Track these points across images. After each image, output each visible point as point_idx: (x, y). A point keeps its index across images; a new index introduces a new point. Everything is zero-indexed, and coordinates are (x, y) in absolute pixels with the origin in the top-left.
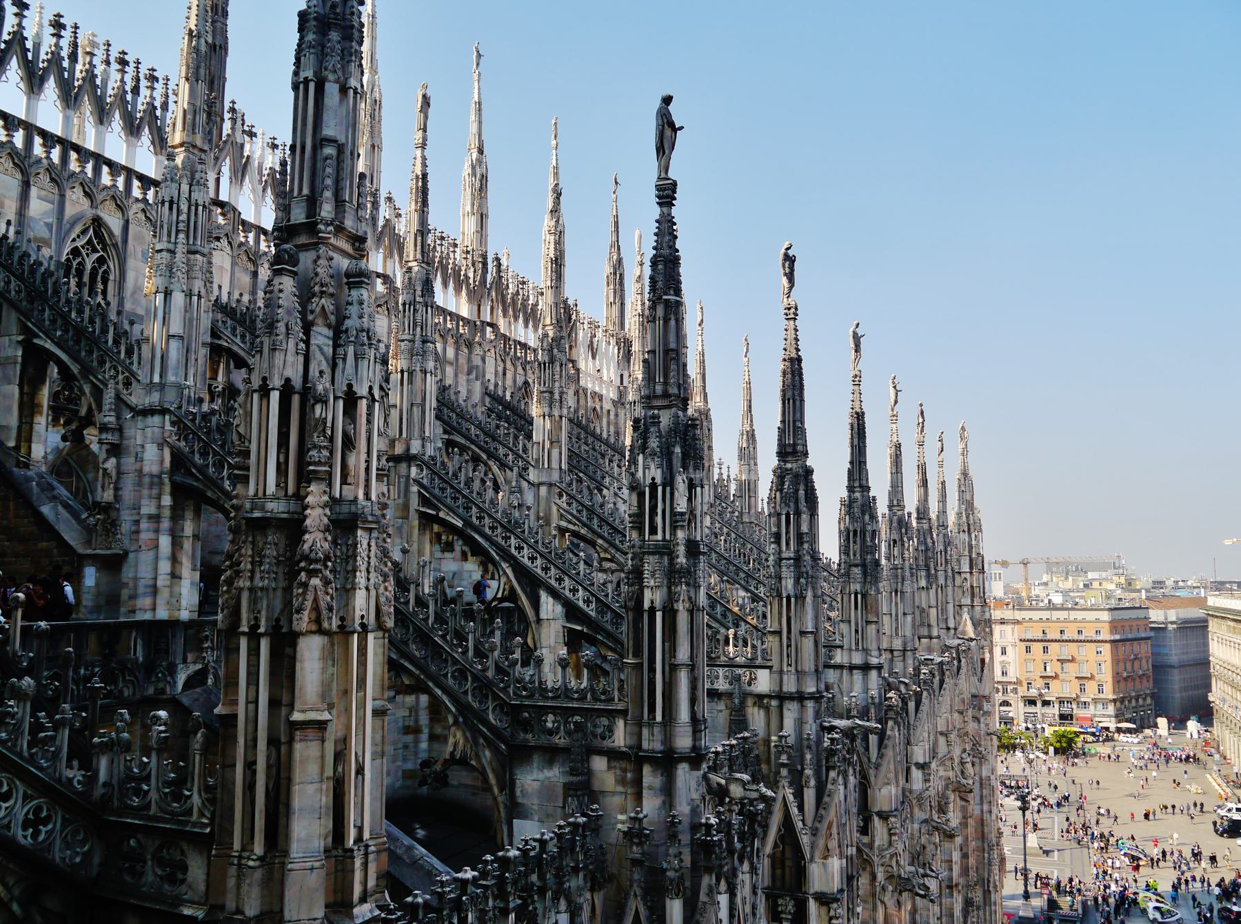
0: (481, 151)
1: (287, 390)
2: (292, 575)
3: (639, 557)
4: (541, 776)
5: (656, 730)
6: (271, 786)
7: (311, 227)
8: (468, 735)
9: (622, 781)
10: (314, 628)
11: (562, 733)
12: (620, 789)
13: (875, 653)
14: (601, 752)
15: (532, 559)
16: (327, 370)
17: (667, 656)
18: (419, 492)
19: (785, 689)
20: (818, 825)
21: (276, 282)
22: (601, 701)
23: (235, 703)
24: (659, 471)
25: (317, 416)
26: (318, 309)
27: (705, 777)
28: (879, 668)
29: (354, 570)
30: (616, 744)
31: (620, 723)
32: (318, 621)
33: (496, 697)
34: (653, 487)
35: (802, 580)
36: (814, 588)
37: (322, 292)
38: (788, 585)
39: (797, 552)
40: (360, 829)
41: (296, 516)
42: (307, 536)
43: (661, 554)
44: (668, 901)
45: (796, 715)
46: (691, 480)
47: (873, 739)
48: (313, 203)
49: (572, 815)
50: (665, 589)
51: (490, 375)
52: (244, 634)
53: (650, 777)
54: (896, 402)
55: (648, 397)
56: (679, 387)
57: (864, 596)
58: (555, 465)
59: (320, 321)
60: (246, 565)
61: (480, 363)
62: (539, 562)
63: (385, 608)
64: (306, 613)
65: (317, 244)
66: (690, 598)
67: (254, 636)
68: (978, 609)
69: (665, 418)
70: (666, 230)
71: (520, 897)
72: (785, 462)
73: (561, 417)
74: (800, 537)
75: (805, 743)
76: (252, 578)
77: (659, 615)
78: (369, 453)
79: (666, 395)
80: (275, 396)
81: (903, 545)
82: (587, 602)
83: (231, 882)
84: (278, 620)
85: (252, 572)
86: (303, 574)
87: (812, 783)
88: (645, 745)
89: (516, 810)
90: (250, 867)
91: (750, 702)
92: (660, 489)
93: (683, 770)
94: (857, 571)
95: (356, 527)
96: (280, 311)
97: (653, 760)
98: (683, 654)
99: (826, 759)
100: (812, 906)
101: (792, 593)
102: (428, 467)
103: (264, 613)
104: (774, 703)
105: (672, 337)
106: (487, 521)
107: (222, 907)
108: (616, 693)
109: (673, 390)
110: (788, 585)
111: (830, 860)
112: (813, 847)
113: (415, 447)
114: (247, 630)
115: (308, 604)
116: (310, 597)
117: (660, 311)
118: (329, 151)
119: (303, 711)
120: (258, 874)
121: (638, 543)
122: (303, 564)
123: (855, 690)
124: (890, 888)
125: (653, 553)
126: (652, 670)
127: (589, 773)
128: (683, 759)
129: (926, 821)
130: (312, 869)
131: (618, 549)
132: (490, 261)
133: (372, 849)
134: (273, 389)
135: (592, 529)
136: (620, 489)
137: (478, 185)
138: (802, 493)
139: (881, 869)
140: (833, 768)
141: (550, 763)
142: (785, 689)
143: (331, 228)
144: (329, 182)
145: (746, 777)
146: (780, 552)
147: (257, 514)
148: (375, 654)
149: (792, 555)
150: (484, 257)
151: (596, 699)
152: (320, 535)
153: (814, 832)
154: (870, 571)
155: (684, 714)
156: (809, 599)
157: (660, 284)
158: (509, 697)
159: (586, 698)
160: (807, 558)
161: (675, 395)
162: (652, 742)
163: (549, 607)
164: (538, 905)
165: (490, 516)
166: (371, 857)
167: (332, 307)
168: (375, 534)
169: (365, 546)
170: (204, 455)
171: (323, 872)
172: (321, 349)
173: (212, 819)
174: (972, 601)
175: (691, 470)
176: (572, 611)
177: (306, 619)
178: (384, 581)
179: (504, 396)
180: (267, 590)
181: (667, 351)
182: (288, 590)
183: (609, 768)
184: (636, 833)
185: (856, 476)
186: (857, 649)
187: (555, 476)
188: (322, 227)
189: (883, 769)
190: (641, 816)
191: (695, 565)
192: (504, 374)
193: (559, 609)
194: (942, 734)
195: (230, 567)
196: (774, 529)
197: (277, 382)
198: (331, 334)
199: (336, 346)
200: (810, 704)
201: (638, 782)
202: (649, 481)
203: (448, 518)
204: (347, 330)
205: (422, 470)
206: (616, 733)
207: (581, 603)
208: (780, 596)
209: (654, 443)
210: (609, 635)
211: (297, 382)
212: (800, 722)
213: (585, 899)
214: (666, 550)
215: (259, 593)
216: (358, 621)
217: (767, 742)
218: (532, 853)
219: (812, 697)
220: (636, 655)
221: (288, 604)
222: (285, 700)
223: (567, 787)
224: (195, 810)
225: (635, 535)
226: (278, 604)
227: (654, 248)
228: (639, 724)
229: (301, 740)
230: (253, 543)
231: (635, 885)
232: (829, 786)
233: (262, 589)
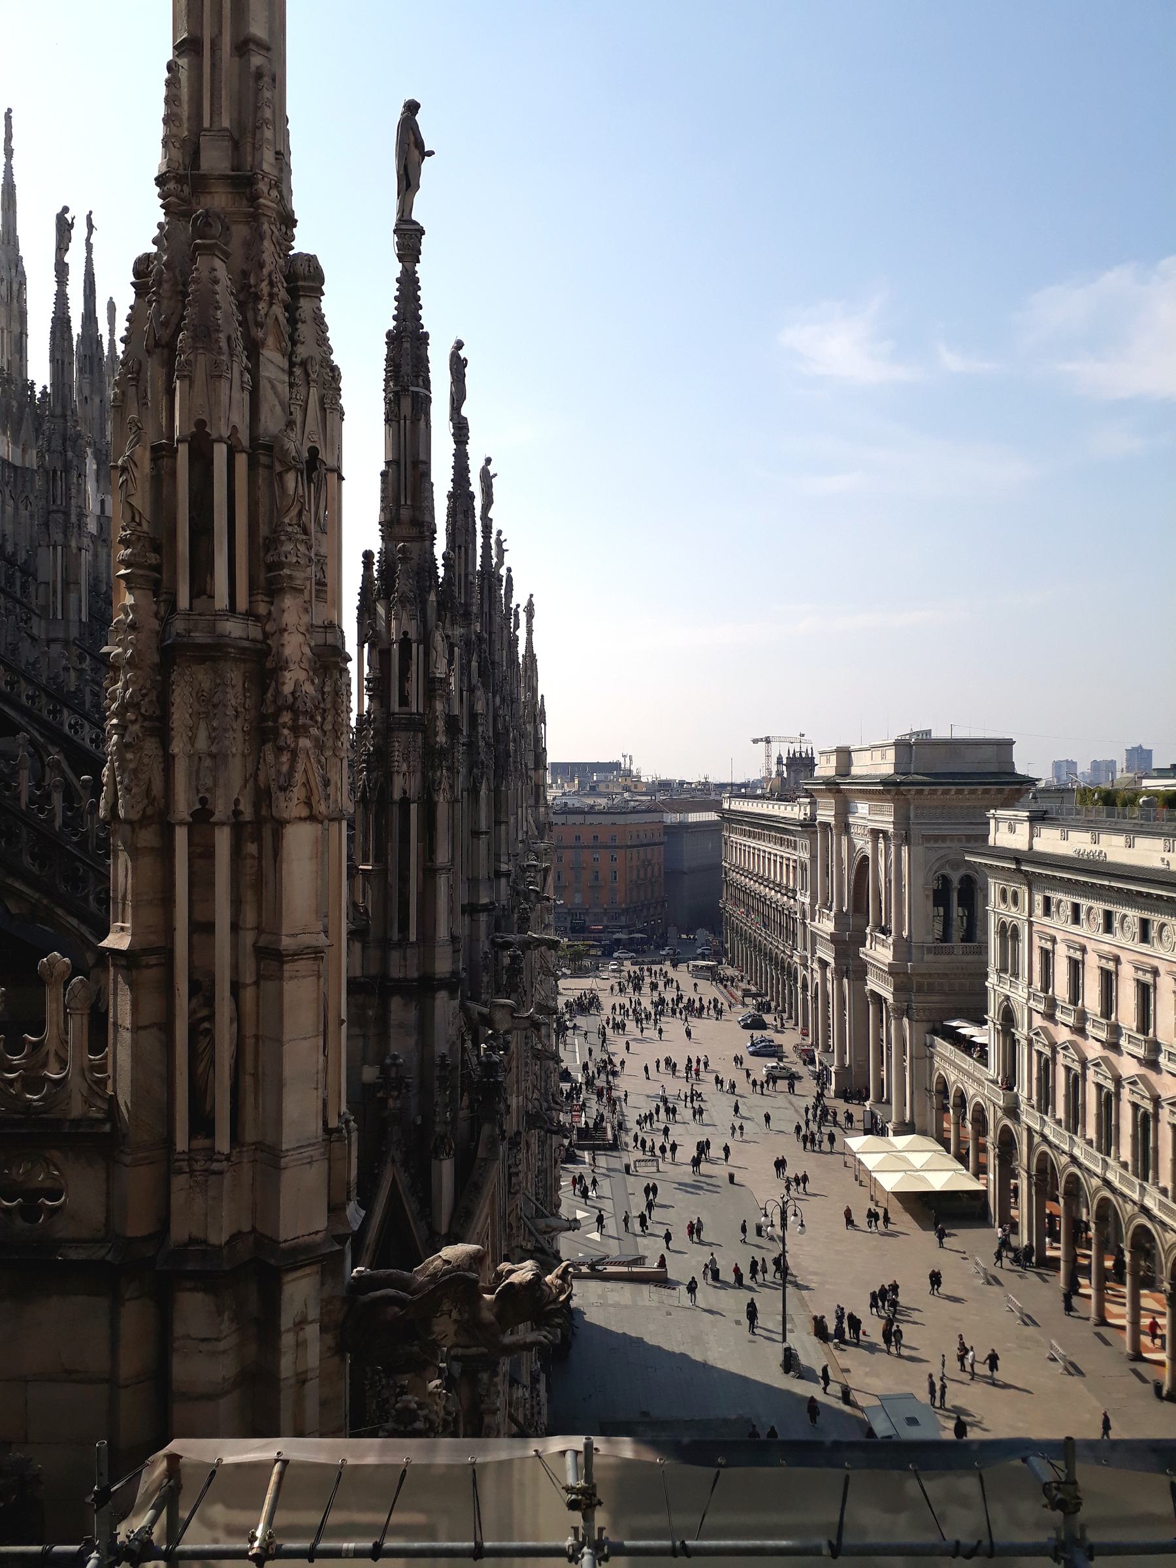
32: (308, 803)
39: (469, 736)
41: (259, 646)
42: (287, 674)
44: (434, 1162)
50: (418, 775)
53: (400, 1011)
58: (73, 616)
60: (180, 717)
90: (214, 1173)
92: (414, 646)
93: (442, 996)
97: (404, 988)
105: (422, 449)
117: (406, 405)
122: (286, 718)
126: (404, 879)
134: (220, 440)
138: (474, 664)
157: (406, 369)
172: (273, 387)
198: (286, 366)
201: (383, 1020)
211: (244, 437)
214: (421, 725)
215: (208, 762)
222: (249, 917)
227: (395, 318)
229: (291, 978)
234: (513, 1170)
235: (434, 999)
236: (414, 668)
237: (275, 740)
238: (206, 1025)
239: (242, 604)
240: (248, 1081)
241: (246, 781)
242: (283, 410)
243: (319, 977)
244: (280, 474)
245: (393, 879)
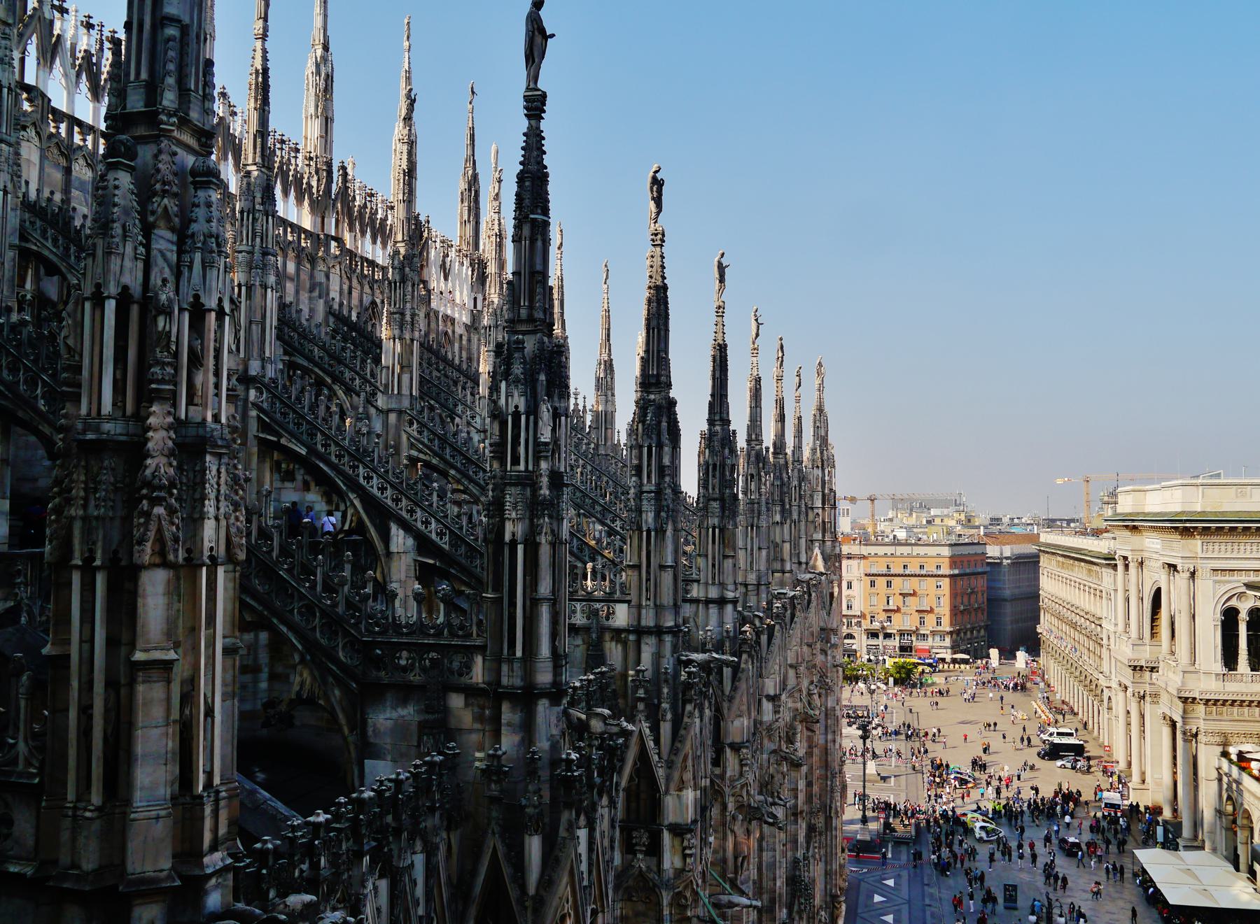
0: (326, 48)
1: (124, 299)
2: (132, 502)
3: (500, 489)
4: (394, 715)
5: (516, 666)
6: (109, 731)
7: (151, 117)
8: (316, 673)
9: (479, 718)
10: (157, 560)
11: (417, 670)
12: (477, 726)
13: (731, 587)
14: (459, 689)
15: (382, 489)
16: (171, 279)
17: (528, 590)
18: (258, 417)
19: (643, 623)
20: (673, 757)
21: (110, 176)
22: (458, 636)
23: (68, 642)
24: (523, 399)
25: (160, 328)
26: (160, 210)
27: (565, 712)
28: (734, 602)
29: (204, 497)
30: (474, 680)
31: (479, 660)
33: (347, 633)
34: (516, 415)
35: (663, 514)
36: (674, 522)
37: (164, 191)
38: (649, 518)
39: (658, 485)
40: (210, 775)
41: (136, 439)
42: (149, 461)
43: (524, 486)
44: (527, 837)
45: (654, 650)
46: (555, 409)
47: (727, 672)
48: (152, 90)
49: (429, 754)
51: (335, 294)
52: (77, 567)
54: (757, 335)
56: (545, 311)
57: (721, 531)
58: (405, 391)
59: (162, 223)
61: (323, 280)
62: (389, 492)
63: (235, 540)
64: (149, 544)
65: (158, 136)
66: (552, 531)
67: (88, 571)
68: (829, 544)
69: (530, 344)
70: (534, 144)
71: (374, 839)
72: (649, 393)
73: (412, 340)
74: (661, 470)
75: (663, 677)
76: (85, 507)
77: (520, 548)
78: (217, 374)
79: (531, 319)
80: (110, 306)
81: (760, 480)
82: (440, 534)
83: (65, 836)
84: (115, 552)
85: (86, 499)
86: (145, 502)
87: (669, 716)
88: (505, 681)
89: (368, 750)
91: (607, 636)
92: (523, 418)
93: (543, 706)
94: (715, 505)
95: (205, 452)
96: (116, 210)
98: (545, 588)
99: (682, 694)
100: (666, 836)
101: (652, 527)
102: (269, 391)
103: (100, 544)
104: (632, 637)
105: (538, 260)
106: (333, 448)
107: (55, 862)
108: (475, 629)
109: (539, 315)
110: (649, 518)
111: (684, 792)
112: (668, 779)
113: (254, 368)
115: (151, 534)
116: (153, 527)
117: (526, 231)
118: (171, 31)
119: (146, 651)
120: (96, 826)
121: (499, 473)
122: (144, 491)
123: (711, 624)
124: (740, 817)
125: (515, 485)
126: (513, 604)
127: (446, 711)
128: (544, 694)
129: (774, 752)
130: (158, 818)
131: (471, 480)
132: (335, 169)
133: (223, 794)
134: (109, 297)
135: (447, 458)
136: (473, 417)
137: (322, 84)
138: (664, 424)
139: (732, 799)
140: (690, 701)
141: (404, 702)
142: (643, 623)
143: (175, 119)
144: (171, 67)
145: (606, 712)
146: (641, 485)
147: (90, 436)
148: (225, 589)
150: (329, 164)
151: (453, 635)
152: (164, 460)
153: (670, 765)
154: (728, 505)
155: (545, 650)
156: (669, 533)
158: (360, 632)
160: (668, 491)
161: (540, 320)
162: (510, 678)
163: (400, 540)
164: (393, 846)
165: (337, 444)
166: (222, 803)
167: (176, 209)
168: (225, 460)
169: (214, 472)
170: (14, 370)
171: (170, 821)
172: (163, 255)
173: (41, 769)
174: (824, 536)
175: (556, 399)
176: (423, 544)
177: (149, 551)
178: (235, 511)
179: (350, 316)
180: (104, 519)
181: (533, 273)
182: (127, 520)
183: (467, 705)
184: (494, 769)
185: (717, 409)
186: (713, 584)
187: (406, 403)
188: (164, 118)
189: (737, 701)
190: (500, 753)
191: (559, 497)
192: (350, 293)
193: (410, 542)
194: (791, 666)
195: (59, 494)
196: (635, 462)
197: (113, 289)
198: (175, 238)
199: (180, 252)
200: (668, 639)
201: (496, 720)
202: (511, 409)
203: (290, 445)
204: (193, 235)
205: (262, 393)
206: (474, 670)
207: (434, 536)
208: (640, 529)
209: (517, 369)
210: (463, 569)
212: (658, 657)
213: (441, 840)
214: (529, 481)
215: (94, 523)
216: (206, 553)
217: (624, 676)
218: (387, 794)
219: (670, 631)
220: (495, 590)
221: (127, 535)
222: (125, 637)
223: (423, 727)
224: (21, 759)
225: (496, 465)
226: (116, 536)
227: (521, 163)
228: (498, 660)
229: (144, 682)
230: (86, 468)
231: (493, 822)
232: (686, 719)
233: (97, 518)
234: (688, 852)
235: (536, 705)
236: (523, 434)
239: (129, 408)
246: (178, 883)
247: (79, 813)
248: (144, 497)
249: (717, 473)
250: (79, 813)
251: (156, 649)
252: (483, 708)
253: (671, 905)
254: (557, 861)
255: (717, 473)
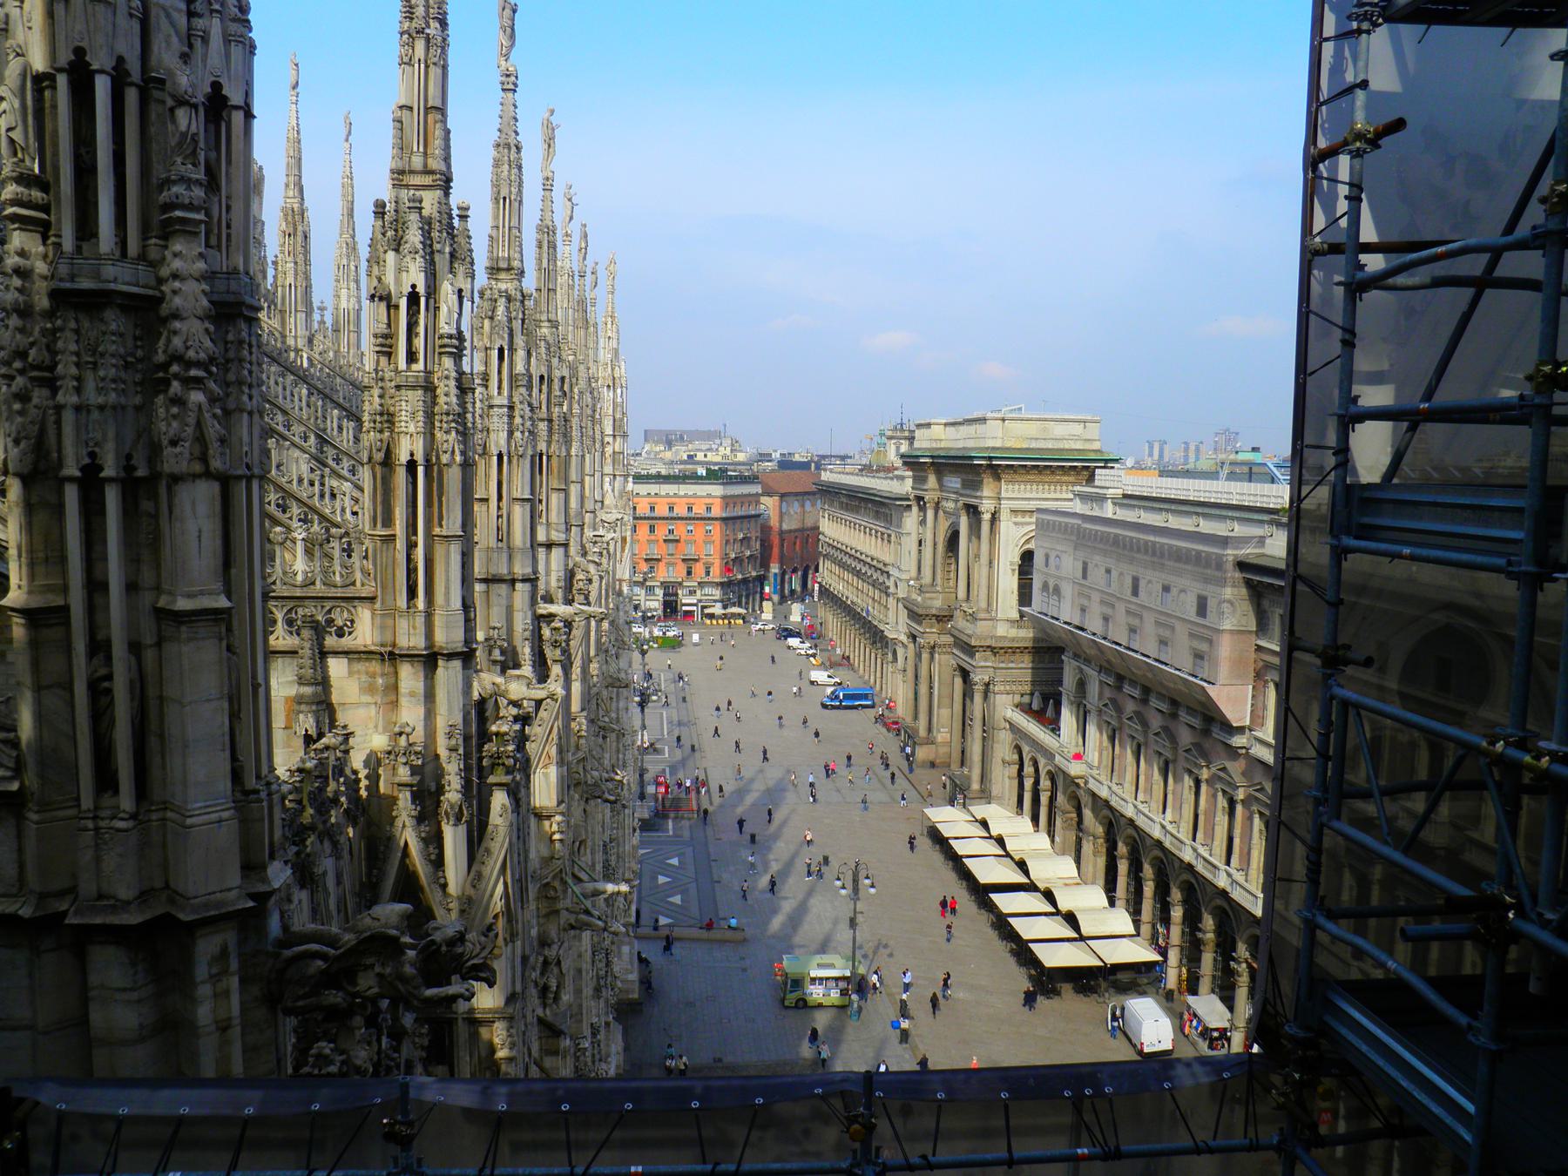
9: (370, 689)
10: (198, 467)
12: (366, 699)
14: (336, 653)
23: (65, 589)
25: (183, 126)
31: (364, 615)
32: (204, 459)
41: (150, 292)
42: (177, 325)
52: (71, 479)
55: (402, 172)
60: (66, 368)
67: (91, 481)
76: (78, 390)
90: (119, 830)
92: (423, 300)
103: (110, 446)
107: (72, 890)
114: (78, 474)
119: (190, 596)
122: (175, 368)
130: (220, 821)
147: (85, 284)
149: (505, 402)
159: (313, 583)
172: (168, 16)
175: (460, 276)
177: (187, 455)
183: (351, 673)
195: (22, 372)
199: (191, 14)
201: (395, 687)
202: (407, 289)
215: (95, 415)
222: (147, 577)
229: (190, 640)
230: (77, 332)
233: (101, 408)
237: (166, 391)
238: (106, 684)
240: (153, 741)
241: (139, 436)
242: (180, 40)
243: (221, 640)
244: (172, 110)
245: (400, 544)
246: (251, 904)
247: (102, 824)
248: (176, 376)
249: (545, 387)
250: (102, 824)
251: (202, 593)
252: (373, 676)
253: (538, 899)
254: (488, 851)
255: (545, 387)
